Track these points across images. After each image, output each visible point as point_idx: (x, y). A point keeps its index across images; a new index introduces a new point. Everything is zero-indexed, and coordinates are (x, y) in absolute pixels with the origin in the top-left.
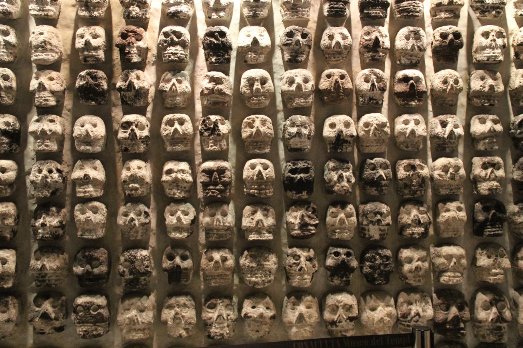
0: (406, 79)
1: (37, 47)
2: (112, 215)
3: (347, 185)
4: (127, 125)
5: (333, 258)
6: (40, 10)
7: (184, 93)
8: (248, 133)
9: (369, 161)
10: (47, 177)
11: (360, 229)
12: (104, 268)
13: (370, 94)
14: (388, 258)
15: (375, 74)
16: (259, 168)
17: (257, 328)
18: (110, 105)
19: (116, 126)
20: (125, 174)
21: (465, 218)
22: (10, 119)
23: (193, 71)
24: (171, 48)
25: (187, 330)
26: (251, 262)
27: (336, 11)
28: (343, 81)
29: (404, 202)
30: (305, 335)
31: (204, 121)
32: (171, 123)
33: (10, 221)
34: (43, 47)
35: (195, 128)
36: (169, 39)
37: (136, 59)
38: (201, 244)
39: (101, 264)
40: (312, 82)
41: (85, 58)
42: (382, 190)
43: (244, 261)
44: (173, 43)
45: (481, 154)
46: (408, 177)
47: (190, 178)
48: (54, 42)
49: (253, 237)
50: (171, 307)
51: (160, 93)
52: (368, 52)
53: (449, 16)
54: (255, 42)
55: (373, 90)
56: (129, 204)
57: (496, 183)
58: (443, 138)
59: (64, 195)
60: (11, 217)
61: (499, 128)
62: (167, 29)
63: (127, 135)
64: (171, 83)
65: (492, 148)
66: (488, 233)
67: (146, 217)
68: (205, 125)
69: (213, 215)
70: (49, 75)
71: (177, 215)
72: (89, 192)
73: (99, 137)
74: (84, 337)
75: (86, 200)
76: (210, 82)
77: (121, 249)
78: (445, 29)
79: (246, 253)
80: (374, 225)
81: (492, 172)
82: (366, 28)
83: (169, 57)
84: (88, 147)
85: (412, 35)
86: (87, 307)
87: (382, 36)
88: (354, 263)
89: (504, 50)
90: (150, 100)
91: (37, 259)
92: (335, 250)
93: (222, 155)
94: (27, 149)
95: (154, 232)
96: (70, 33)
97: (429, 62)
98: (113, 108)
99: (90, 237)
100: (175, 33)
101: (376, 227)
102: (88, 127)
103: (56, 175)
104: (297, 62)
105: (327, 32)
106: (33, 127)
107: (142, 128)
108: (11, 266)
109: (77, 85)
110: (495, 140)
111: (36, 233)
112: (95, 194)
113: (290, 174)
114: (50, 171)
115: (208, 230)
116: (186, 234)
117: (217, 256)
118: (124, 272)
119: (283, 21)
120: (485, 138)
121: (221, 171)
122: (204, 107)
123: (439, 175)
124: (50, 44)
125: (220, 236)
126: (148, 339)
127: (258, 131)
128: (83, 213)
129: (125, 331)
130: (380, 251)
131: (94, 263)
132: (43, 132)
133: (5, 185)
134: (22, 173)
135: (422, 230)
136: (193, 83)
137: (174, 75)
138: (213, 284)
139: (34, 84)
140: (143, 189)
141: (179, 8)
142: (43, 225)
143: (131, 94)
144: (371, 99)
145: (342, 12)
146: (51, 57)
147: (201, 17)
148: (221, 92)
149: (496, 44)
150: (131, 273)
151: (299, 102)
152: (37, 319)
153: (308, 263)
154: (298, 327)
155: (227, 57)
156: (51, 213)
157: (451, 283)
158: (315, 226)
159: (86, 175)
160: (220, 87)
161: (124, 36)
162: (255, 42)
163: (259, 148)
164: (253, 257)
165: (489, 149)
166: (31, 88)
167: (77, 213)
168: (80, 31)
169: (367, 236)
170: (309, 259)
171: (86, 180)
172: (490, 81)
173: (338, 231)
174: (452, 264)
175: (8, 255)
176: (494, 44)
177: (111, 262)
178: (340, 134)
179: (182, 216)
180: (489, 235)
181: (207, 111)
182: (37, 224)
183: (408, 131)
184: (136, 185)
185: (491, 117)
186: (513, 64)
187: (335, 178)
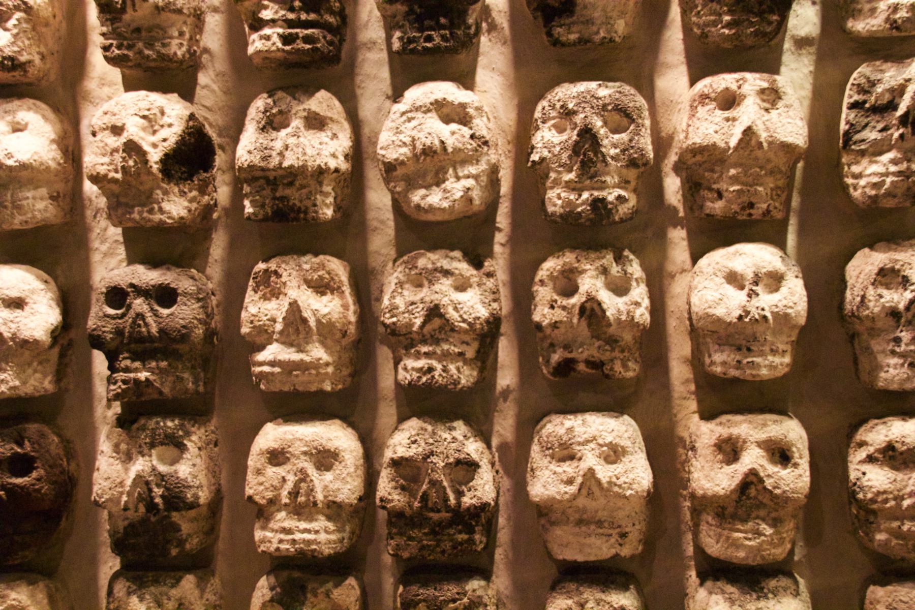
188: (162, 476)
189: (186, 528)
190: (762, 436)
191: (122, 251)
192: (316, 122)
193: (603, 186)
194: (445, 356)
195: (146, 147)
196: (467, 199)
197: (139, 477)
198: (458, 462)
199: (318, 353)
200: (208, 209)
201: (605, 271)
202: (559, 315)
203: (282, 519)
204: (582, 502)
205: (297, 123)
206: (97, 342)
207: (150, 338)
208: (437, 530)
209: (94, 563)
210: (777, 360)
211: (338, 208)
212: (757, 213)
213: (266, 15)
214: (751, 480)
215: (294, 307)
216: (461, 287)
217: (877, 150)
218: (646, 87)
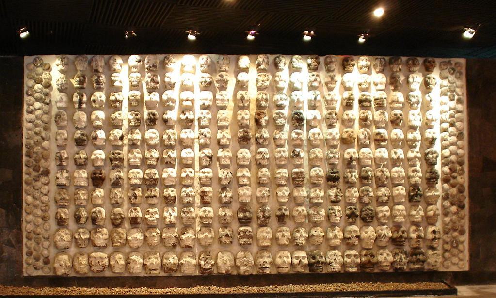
0: (379, 134)
11: (360, 198)
21: (405, 194)
40: (339, 135)
43: (311, 212)
44: (280, 117)
47: (287, 176)
50: (280, 231)
63: (261, 157)
75: (242, 186)
82: (362, 111)
86: (244, 232)
92: (350, 207)
100: (280, 113)
103: (230, 175)
107: (267, 154)
114: (228, 173)
117: (300, 209)
119: (326, 107)
135: (387, 198)
142: (226, 196)
152: (223, 237)
158: (342, 196)
160: (301, 136)
179: (285, 192)
184: (265, 179)
187: (350, 176)
203: (133, 180)
213: (132, 121)
214: (187, 175)
216: (155, 153)
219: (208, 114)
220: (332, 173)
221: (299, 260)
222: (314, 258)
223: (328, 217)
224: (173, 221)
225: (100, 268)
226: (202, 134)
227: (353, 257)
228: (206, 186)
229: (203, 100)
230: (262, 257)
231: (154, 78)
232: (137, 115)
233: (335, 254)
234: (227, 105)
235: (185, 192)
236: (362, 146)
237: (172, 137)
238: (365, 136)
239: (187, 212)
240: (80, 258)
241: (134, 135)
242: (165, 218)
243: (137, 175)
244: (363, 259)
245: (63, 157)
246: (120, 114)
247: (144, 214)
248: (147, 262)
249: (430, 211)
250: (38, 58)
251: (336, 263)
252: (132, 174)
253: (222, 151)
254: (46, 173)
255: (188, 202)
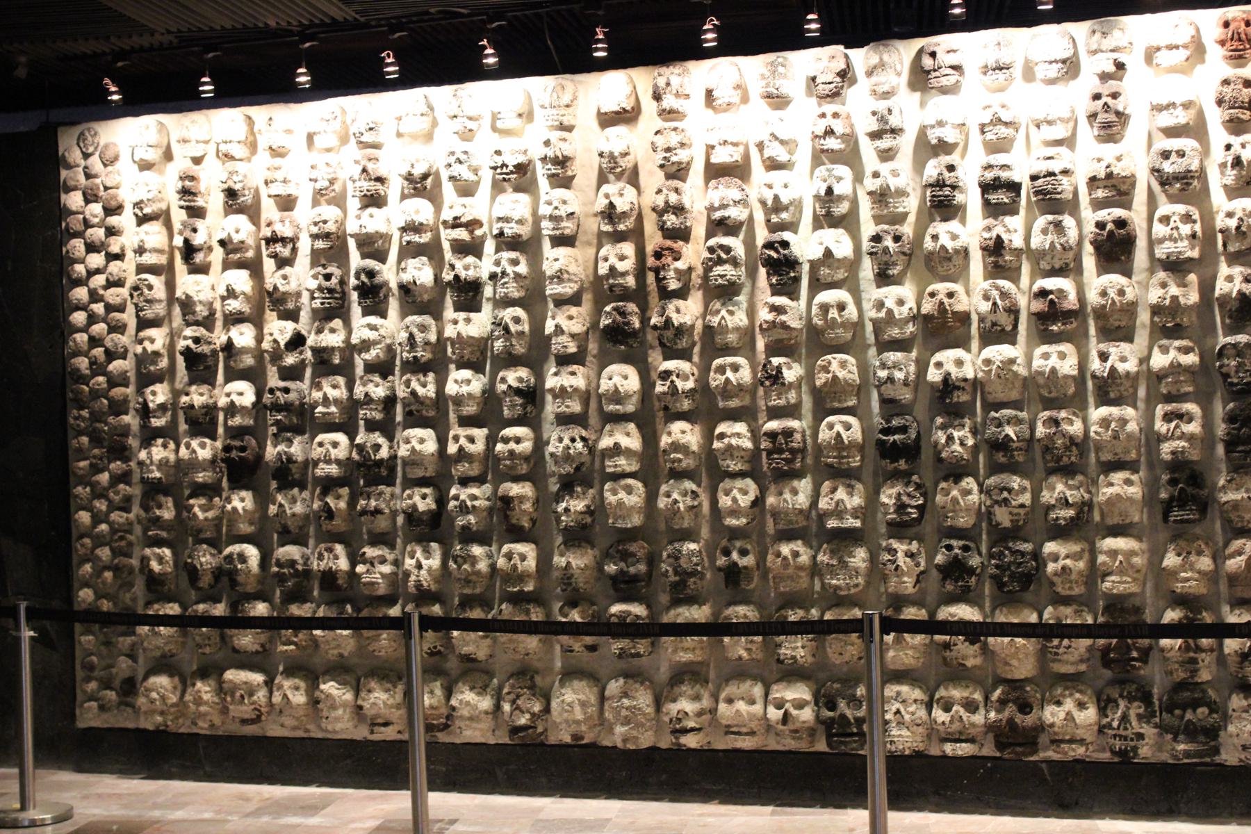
0: (1043, 293)
1: (552, 278)
2: (651, 497)
3: (959, 449)
4: (666, 375)
5: (943, 553)
6: (554, 229)
7: (737, 329)
8: (823, 381)
9: (993, 414)
10: (569, 448)
12: (642, 567)
13: (992, 318)
14: (1023, 554)
15: (997, 288)
16: (839, 428)
17: (839, 650)
18: (645, 347)
19: (654, 375)
20: (665, 441)
22: (523, 372)
23: (752, 295)
24: (719, 268)
25: (748, 650)
26: (831, 558)
27: (940, 201)
28: (951, 301)
29: (1051, 472)
30: (906, 661)
31: (765, 365)
32: (721, 369)
33: (527, 506)
34: (558, 277)
35: (754, 372)
36: (714, 256)
37: (673, 285)
38: (769, 535)
39: (638, 561)
41: (611, 287)
42: (1012, 456)
43: (822, 558)
44: (720, 262)
45: (1169, 399)
46: (1050, 437)
47: (748, 444)
48: (573, 268)
49: (832, 523)
51: (708, 329)
52: (990, 256)
53: (1109, 194)
54: (828, 253)
55: (995, 312)
56: (672, 481)
57: (1183, 443)
58: (1103, 377)
59: (592, 471)
60: (528, 500)
61: (1191, 359)
62: (712, 242)
63: (665, 388)
64: (720, 316)
65: (1178, 391)
66: (1172, 519)
67: (694, 499)
68: (767, 372)
69: (781, 494)
70: (568, 313)
71: (732, 495)
72: (620, 465)
73: (632, 393)
74: (620, 656)
75: (617, 477)
76: (771, 311)
77: (665, 541)
78: (1103, 215)
79: (825, 546)
80: (1000, 506)
81: (1177, 427)
83: (716, 280)
84: (618, 407)
85: (1051, 227)
87: (1009, 231)
88: (975, 561)
89: (1196, 242)
90: (696, 338)
91: (562, 555)
93: (792, 411)
94: (545, 411)
95: (707, 518)
96: (592, 251)
97: (1089, 262)
98: (650, 351)
99: (624, 526)
100: (722, 247)
101: (1004, 509)
102: (617, 380)
103: (579, 445)
104: (888, 277)
105: (931, 231)
106: (551, 382)
107: (686, 378)
108: (531, 564)
109: (601, 325)
110: (1182, 378)
111: (558, 521)
112: (628, 469)
113: (880, 436)
114: (573, 440)
115: (776, 514)
116: (744, 521)
117: (785, 549)
118: (667, 571)
120: (1166, 376)
121: (788, 433)
122: (766, 346)
123: (1095, 432)
124: (568, 272)
125: (791, 522)
126: (699, 663)
127: (835, 378)
128: (615, 493)
129: (670, 650)
130: (1010, 544)
131: (630, 560)
132: (563, 389)
133: (520, 459)
134: (540, 444)
135: (1071, 513)
136: (751, 313)
137: (723, 304)
138: (782, 589)
139: (549, 327)
140: (688, 461)
141: (726, 213)
142: (567, 510)
143: (669, 334)
144: (994, 324)
145: (949, 200)
146: (568, 289)
147: (759, 217)
148: (784, 326)
149: (1180, 235)
150: (676, 573)
151: (895, 332)
153: (908, 560)
154: (896, 650)
155: (792, 275)
156: (575, 495)
157: (1115, 591)
159: (616, 444)
160: (783, 318)
161: (658, 255)
162: (828, 253)
163: (840, 401)
164: (833, 553)
165: (1174, 392)
166: (547, 332)
167: (607, 494)
168: (603, 252)
169: (994, 523)
170: (910, 555)
171: (616, 450)
172: (1174, 290)
173: (950, 515)
174: (1117, 563)
175: (527, 549)
176: (1176, 234)
177: (652, 560)
178: (947, 377)
179: (739, 496)
180: (1175, 521)
181: (773, 350)
182: (559, 510)
183: (1047, 370)
184: (679, 456)
185: (1177, 343)
186: (1223, 258)
187: (943, 441)
188: (285, 452)
189: (294, 470)
190: (465, 434)
191: (277, 375)
192: (333, 331)
193: (417, 352)
194: (371, 409)
195: (279, 340)
196: (377, 356)
197: (279, 453)
198: (375, 445)
199: (333, 409)
200: (303, 361)
201: (418, 380)
202: (406, 395)
203: (321, 465)
204: (413, 457)
205: (326, 331)
206: (265, 407)
207: (281, 405)
208: (369, 468)
209: (268, 486)
210: (469, 409)
211: (342, 359)
212: (466, 357)
213: (316, 295)
214: (461, 449)
215: (325, 395)
216: (377, 386)
217: (498, 338)
218: (438, 317)
219: (515, 262)
220: (886, 431)
221: (783, 711)
222: (832, 706)
223: (877, 571)
224: (425, 584)
225: (245, 710)
226: (499, 325)
227: (954, 708)
228: (517, 479)
229: (500, 219)
230: (674, 700)
231: (370, 166)
232: (328, 277)
233: (898, 693)
234: (567, 232)
235: (456, 498)
236: (995, 334)
237: (419, 337)
238: (995, 304)
239: (460, 556)
240: (199, 685)
241: (322, 336)
242: (407, 574)
243: (336, 445)
244: (992, 715)
245: (151, 405)
246: (285, 277)
247: (353, 564)
248: (364, 700)
249: (1232, 556)
250: (89, 130)
251: (901, 723)
252: (319, 450)
253: (556, 374)
254: (120, 451)
255: (466, 528)
